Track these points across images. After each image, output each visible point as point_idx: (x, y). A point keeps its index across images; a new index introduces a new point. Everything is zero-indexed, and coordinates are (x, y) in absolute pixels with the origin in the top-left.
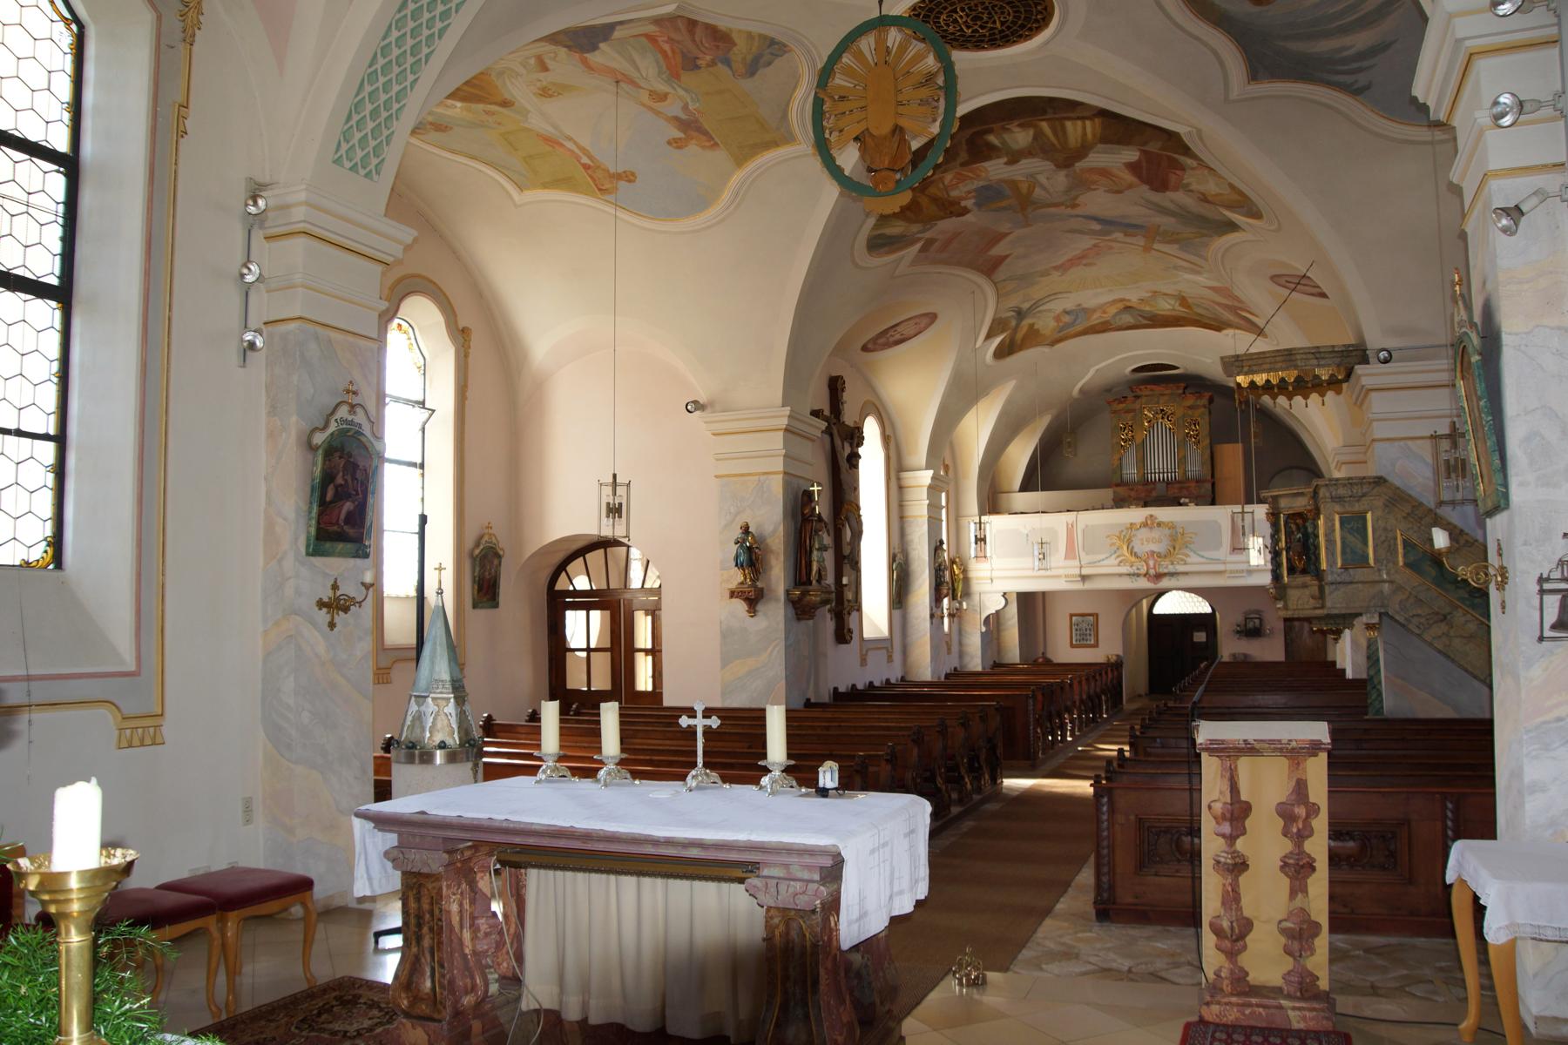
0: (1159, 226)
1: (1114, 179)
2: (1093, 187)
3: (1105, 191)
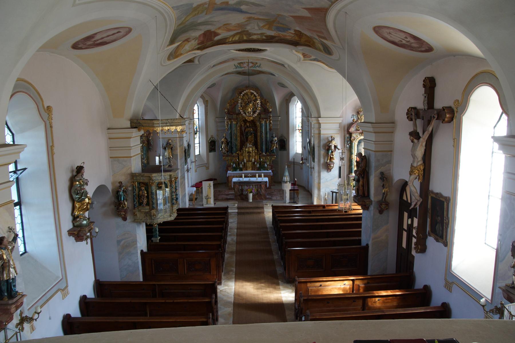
0: (206, 14)
1: (226, 29)
2: (237, 25)
3: (232, 24)
